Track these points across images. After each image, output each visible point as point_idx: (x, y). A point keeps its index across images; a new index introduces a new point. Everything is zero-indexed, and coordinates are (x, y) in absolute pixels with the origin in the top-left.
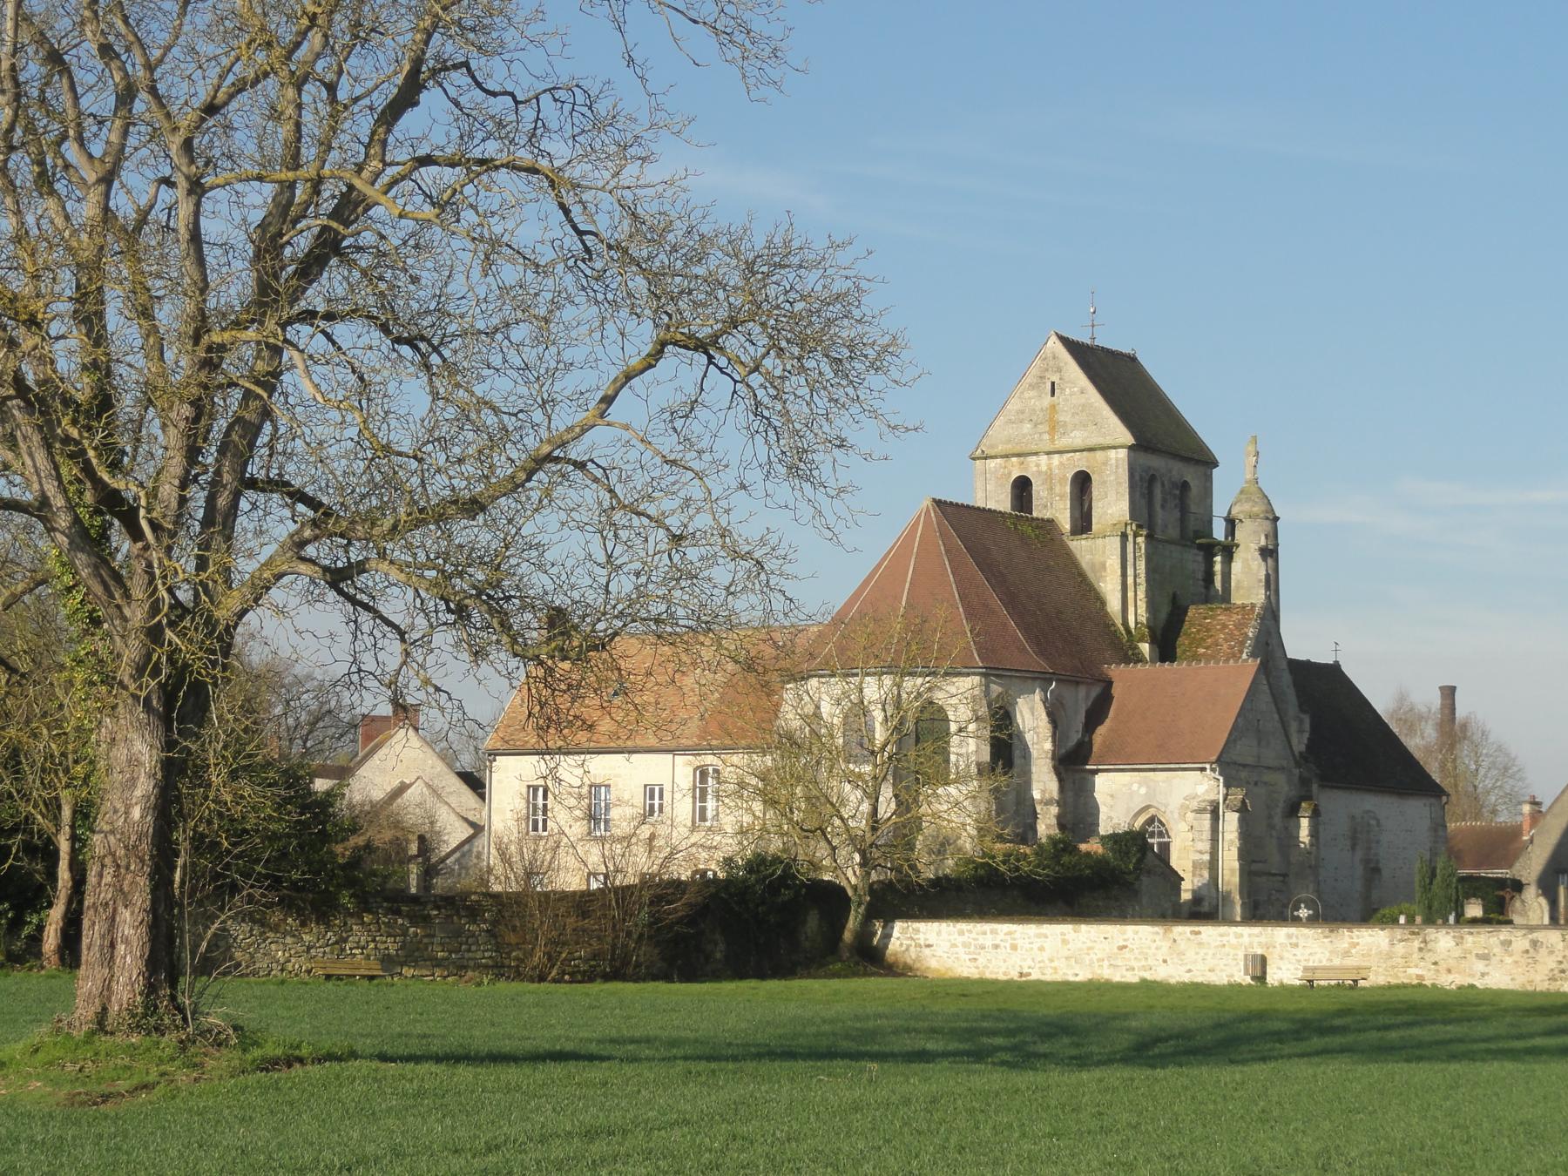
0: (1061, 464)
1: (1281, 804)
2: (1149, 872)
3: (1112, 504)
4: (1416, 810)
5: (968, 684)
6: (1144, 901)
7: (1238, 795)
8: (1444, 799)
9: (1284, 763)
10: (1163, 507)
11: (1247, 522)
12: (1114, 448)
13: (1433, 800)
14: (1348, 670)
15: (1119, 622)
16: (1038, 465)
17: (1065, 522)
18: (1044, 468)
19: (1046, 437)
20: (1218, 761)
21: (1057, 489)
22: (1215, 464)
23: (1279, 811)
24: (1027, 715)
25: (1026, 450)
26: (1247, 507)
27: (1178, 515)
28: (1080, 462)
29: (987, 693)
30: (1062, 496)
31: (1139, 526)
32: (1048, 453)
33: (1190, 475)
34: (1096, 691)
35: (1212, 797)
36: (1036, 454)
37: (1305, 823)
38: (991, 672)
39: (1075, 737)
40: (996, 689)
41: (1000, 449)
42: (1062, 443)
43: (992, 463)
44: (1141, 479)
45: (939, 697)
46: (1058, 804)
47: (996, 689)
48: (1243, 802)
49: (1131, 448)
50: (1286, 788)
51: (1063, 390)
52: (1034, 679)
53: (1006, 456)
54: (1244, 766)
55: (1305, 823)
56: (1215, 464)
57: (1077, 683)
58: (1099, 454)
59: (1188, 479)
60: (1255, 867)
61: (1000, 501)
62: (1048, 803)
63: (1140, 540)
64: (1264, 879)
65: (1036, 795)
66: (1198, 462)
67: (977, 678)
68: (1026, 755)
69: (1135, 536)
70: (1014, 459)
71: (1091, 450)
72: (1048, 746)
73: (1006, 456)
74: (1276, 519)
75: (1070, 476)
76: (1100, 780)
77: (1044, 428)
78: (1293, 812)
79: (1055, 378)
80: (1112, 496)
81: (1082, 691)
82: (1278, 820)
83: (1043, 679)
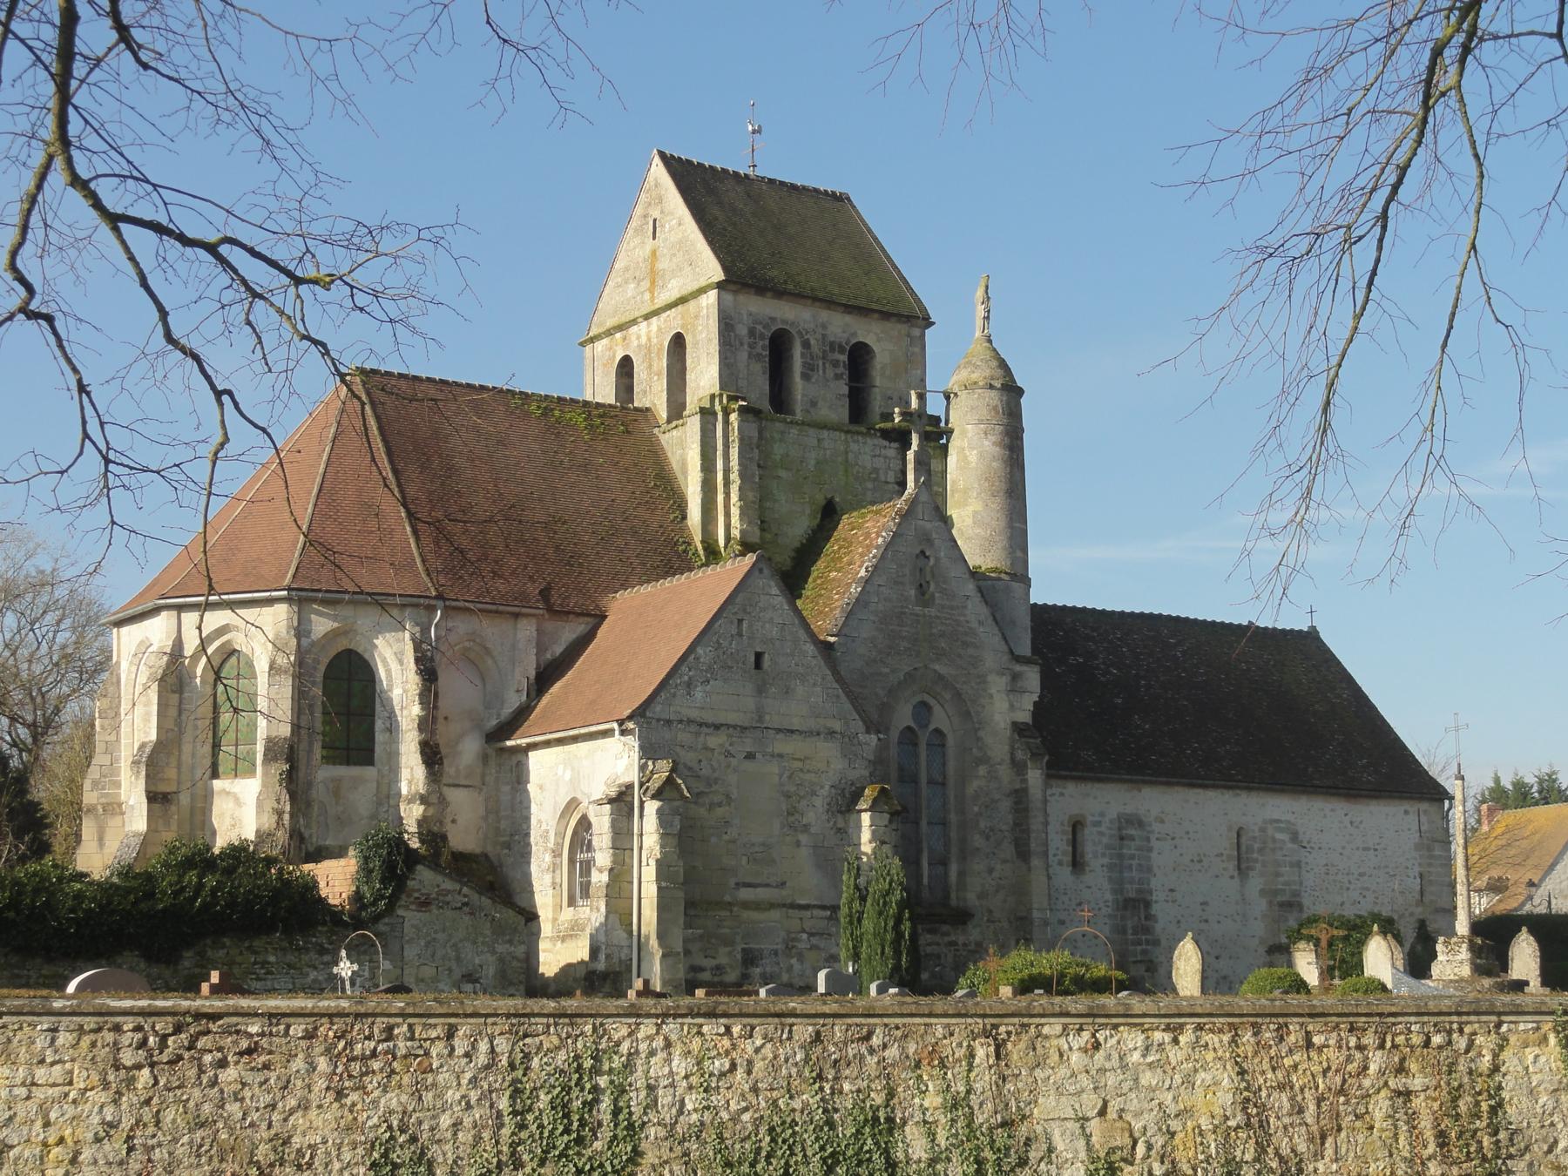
0: (659, 329)
1: (825, 791)
2: (424, 904)
3: (704, 376)
4: (1388, 823)
5: (276, 618)
6: (410, 952)
7: (663, 768)
8: (1447, 803)
9: (837, 726)
10: (806, 377)
11: (963, 395)
12: (702, 291)
13: (1424, 806)
14: (1325, 637)
15: (697, 538)
16: (638, 338)
17: (662, 413)
18: (644, 340)
19: (647, 296)
20: (639, 714)
21: (655, 368)
22: (928, 323)
23: (819, 802)
24: (394, 666)
25: (624, 319)
26: (963, 375)
27: (845, 390)
28: (672, 322)
29: (300, 631)
30: (659, 374)
31: (730, 398)
32: (647, 317)
33: (870, 333)
34: (569, 632)
35: (626, 779)
36: (634, 322)
37: (866, 818)
38: (301, 597)
39: (514, 701)
40: (321, 625)
41: (610, 323)
42: (659, 303)
43: (600, 346)
44: (752, 332)
45: (238, 641)
46: (424, 800)
47: (321, 625)
48: (669, 781)
49: (720, 286)
50: (838, 764)
51: (663, 226)
52: (404, 606)
53: (609, 333)
54: (717, 727)
55: (866, 818)
56: (928, 323)
57: (517, 616)
58: (692, 304)
59: (869, 340)
60: (745, 894)
61: (602, 390)
62: (410, 801)
63: (733, 417)
64: (775, 914)
65: (404, 791)
66: (886, 316)
67: (282, 609)
68: (392, 728)
69: (726, 413)
70: (618, 335)
71: (683, 300)
72: (416, 710)
73: (609, 333)
74: (1020, 392)
75: (666, 344)
76: (538, 762)
77: (646, 284)
78: (846, 803)
79: (656, 214)
80: (704, 358)
81: (526, 630)
82: (815, 814)
83: (417, 604)
